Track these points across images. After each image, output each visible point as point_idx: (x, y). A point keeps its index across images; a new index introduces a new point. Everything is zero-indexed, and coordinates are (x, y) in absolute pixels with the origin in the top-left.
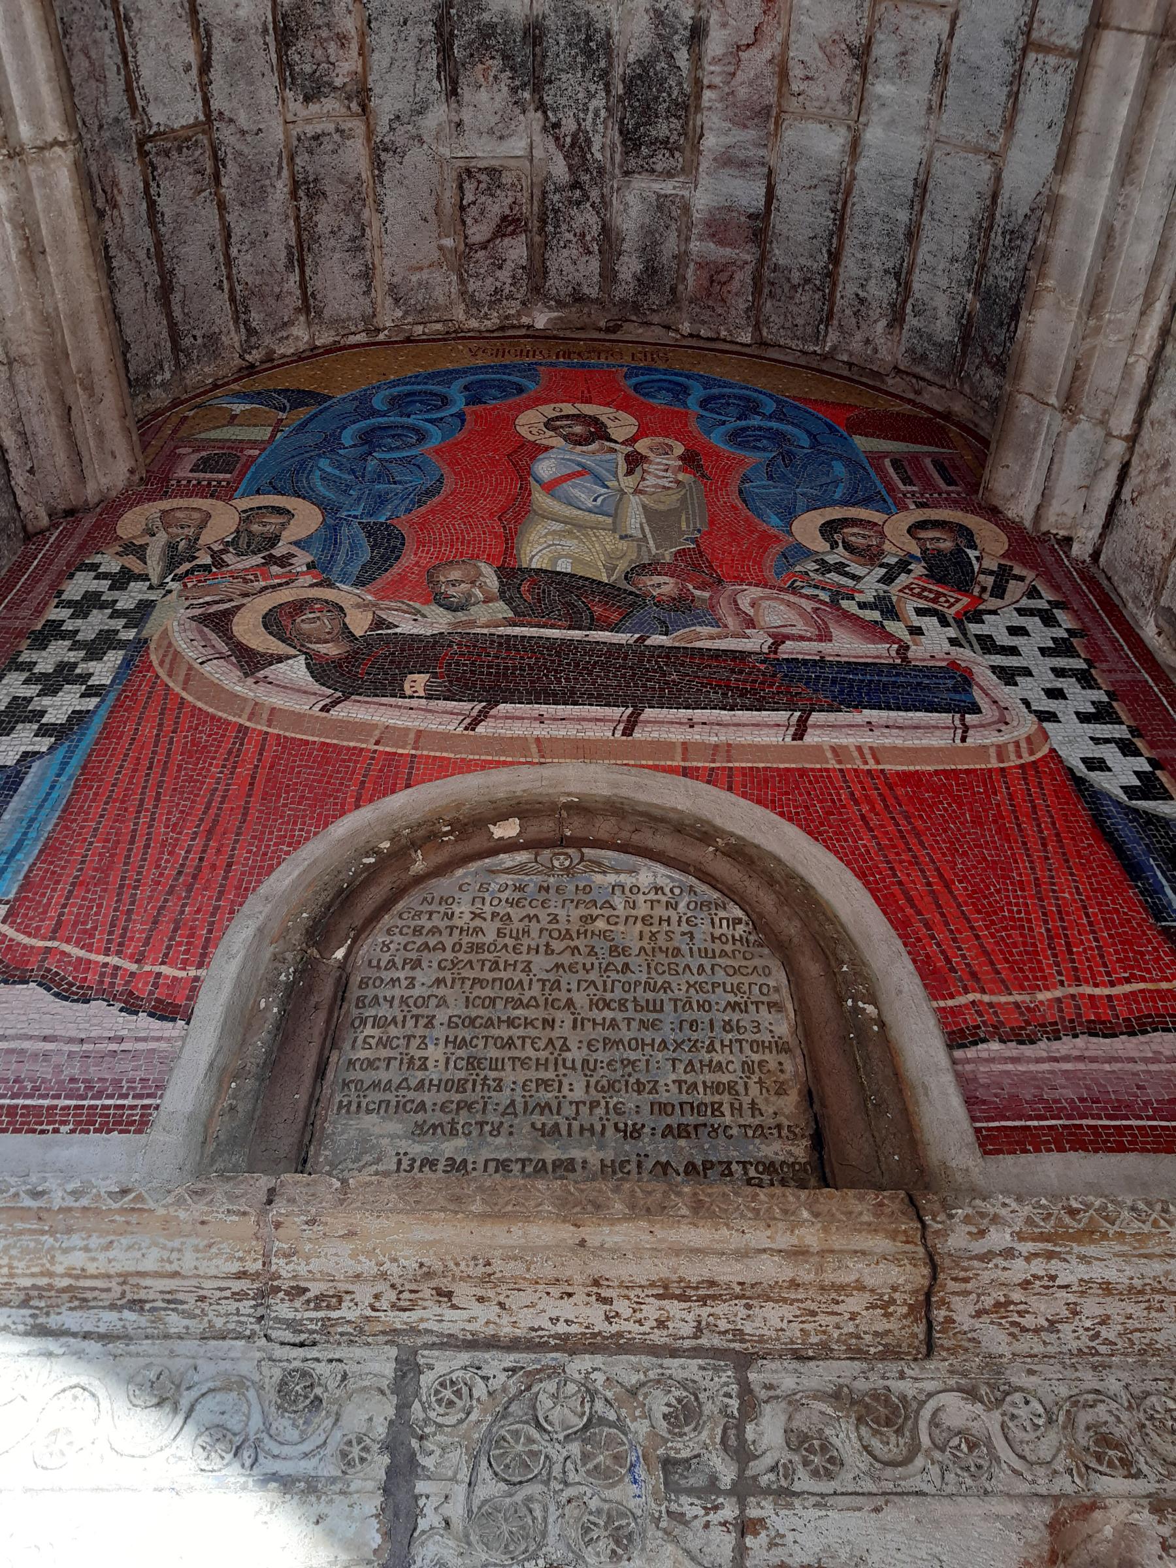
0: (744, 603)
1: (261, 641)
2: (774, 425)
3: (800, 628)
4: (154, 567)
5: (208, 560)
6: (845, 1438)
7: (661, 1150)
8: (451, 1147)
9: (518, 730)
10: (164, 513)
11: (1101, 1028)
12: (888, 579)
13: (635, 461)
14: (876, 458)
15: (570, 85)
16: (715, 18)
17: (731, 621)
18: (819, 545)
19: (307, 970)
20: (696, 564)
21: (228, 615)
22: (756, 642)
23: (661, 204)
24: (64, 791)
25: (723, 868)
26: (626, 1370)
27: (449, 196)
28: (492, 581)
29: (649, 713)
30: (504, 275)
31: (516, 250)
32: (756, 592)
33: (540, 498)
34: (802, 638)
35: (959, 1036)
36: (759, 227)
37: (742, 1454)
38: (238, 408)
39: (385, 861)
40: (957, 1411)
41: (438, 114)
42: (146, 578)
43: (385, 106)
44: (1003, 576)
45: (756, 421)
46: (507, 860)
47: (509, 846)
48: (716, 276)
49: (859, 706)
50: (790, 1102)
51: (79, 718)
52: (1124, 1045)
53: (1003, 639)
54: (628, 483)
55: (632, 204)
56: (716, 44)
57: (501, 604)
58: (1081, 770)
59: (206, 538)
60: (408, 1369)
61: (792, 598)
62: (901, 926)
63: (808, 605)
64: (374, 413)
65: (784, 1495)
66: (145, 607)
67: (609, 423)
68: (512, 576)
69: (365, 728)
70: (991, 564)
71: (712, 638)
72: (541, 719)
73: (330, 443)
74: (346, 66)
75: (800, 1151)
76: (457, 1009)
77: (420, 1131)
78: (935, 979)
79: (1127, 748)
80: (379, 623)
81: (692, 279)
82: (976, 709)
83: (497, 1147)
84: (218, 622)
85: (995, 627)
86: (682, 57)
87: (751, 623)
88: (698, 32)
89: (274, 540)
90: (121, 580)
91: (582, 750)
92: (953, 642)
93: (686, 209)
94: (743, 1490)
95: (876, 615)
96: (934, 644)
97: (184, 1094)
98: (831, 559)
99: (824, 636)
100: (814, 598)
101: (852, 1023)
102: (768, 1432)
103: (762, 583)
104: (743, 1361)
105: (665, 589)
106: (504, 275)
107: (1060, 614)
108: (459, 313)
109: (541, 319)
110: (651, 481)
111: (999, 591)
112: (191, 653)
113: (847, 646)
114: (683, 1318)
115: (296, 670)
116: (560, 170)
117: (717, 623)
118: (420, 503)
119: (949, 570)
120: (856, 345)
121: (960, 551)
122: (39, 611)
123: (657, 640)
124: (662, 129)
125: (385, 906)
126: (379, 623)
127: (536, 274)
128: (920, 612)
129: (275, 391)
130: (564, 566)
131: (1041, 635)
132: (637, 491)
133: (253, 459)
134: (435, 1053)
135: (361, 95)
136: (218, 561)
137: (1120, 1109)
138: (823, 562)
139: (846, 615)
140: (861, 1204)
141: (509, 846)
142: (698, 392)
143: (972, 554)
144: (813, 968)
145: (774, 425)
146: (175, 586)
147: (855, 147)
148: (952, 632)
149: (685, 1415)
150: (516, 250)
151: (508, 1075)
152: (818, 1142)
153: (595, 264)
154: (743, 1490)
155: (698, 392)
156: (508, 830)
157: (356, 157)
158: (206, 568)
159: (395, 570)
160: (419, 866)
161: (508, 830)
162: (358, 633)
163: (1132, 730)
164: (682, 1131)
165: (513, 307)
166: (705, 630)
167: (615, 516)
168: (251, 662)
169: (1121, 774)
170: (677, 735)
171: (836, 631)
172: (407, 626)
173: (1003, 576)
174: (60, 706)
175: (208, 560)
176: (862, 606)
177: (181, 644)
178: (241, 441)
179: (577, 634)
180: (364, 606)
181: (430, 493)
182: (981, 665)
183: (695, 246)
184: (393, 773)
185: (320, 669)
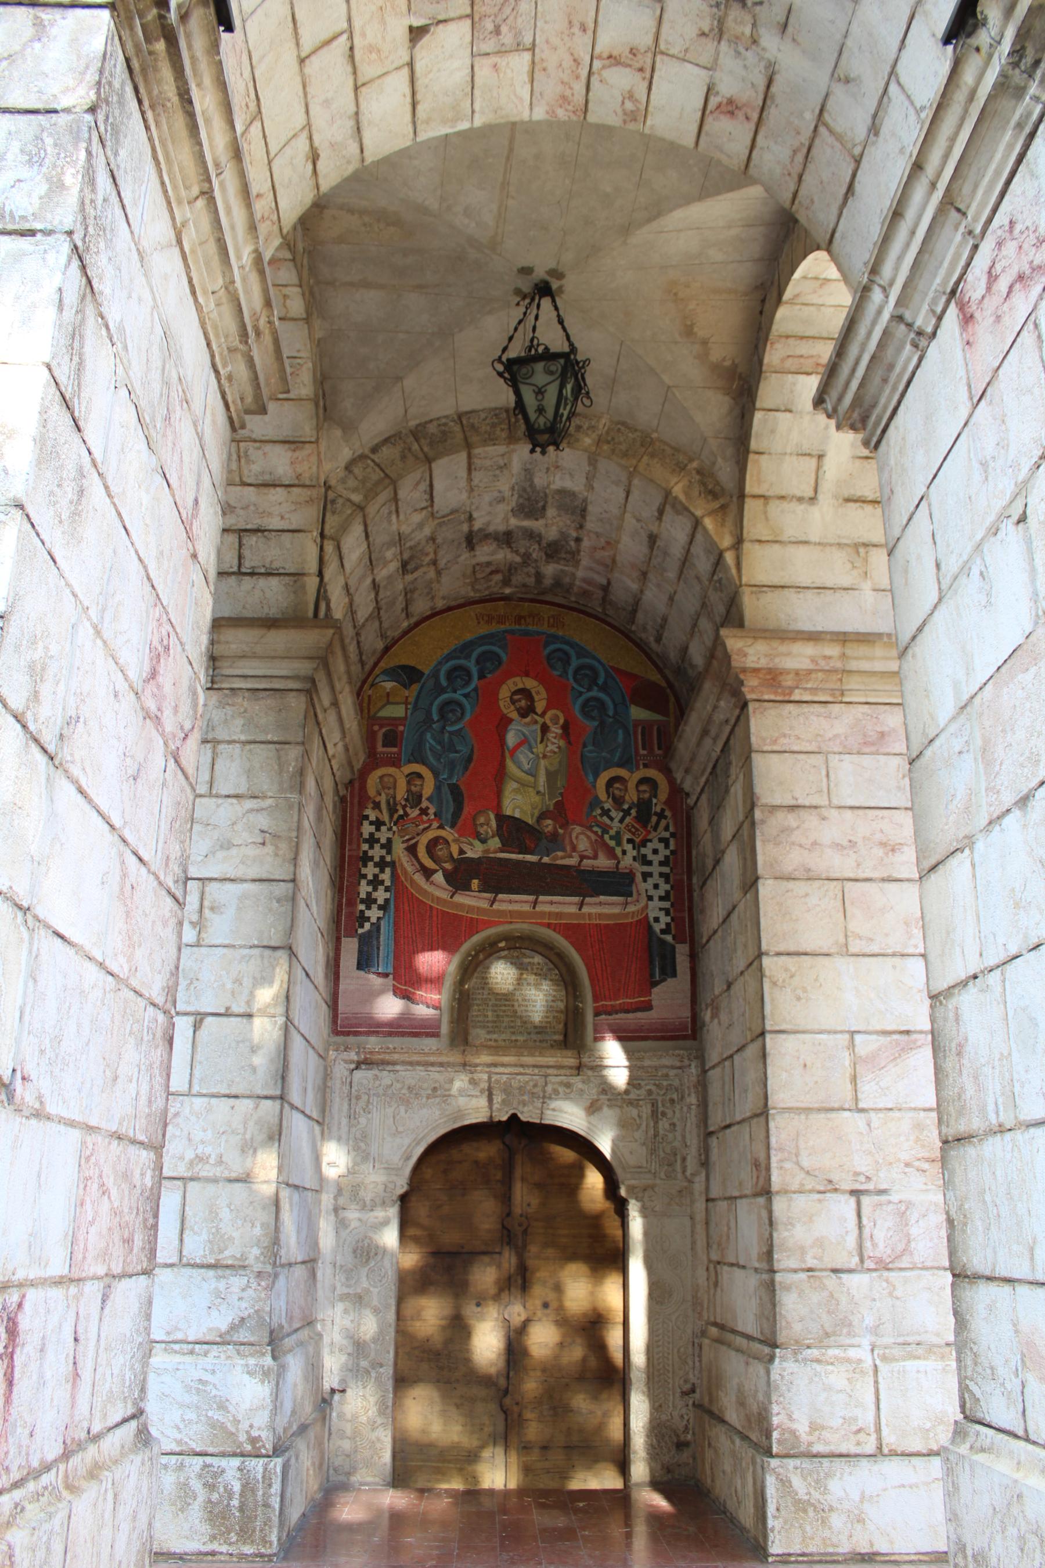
0: (574, 835)
1: (429, 863)
2: (602, 696)
3: (590, 853)
4: (386, 817)
5: (401, 812)
6: (561, 1089)
7: (534, 1037)
8: (495, 1036)
9: (504, 907)
10: (381, 778)
11: (627, 1011)
12: (621, 821)
13: (545, 729)
14: (637, 723)
15: (523, 545)
16: (585, 539)
17: (568, 848)
18: (602, 795)
19: (461, 993)
20: (560, 813)
21: (415, 845)
22: (573, 861)
23: (562, 571)
24: (392, 933)
25: (555, 959)
26: (527, 1078)
27: (469, 571)
28: (494, 823)
29: (541, 898)
30: (493, 583)
31: (498, 577)
32: (578, 829)
33: (511, 766)
34: (588, 858)
35: (597, 1014)
36: (606, 588)
37: (544, 1092)
38: (389, 685)
39: (474, 957)
40: (580, 1085)
41: (465, 555)
42: (384, 824)
43: (442, 563)
44: (661, 815)
45: (595, 693)
46: (503, 953)
47: (502, 949)
48: (585, 593)
49: (598, 895)
50: (561, 1026)
51: (387, 901)
52: (630, 1016)
53: (651, 857)
54: (541, 747)
55: (550, 570)
56: (586, 543)
57: (497, 839)
58: (651, 920)
59: (399, 797)
60: (490, 1078)
61: (589, 833)
62: (592, 980)
63: (593, 837)
64: (440, 690)
65: (550, 1098)
66: (389, 840)
67: (536, 698)
68: (501, 818)
69: (461, 906)
70: (658, 810)
71: (562, 858)
72: (510, 902)
73: (428, 720)
74: (427, 559)
75: (560, 1038)
76: (493, 1002)
77: (489, 1033)
78: (596, 998)
79: (667, 913)
80: (462, 852)
81: (576, 589)
82: (631, 895)
83: (504, 1037)
84: (412, 850)
85: (647, 851)
86: (572, 543)
87: (574, 848)
88: (578, 540)
89: (421, 796)
90: (378, 824)
91: (521, 915)
92: (634, 859)
93: (573, 574)
94: (544, 1097)
95: (612, 843)
96: (627, 862)
97: (445, 1029)
98: (607, 806)
99: (595, 857)
100: (596, 833)
101: (576, 1008)
102: (549, 1088)
103: (582, 826)
104: (546, 1076)
105: (550, 828)
106: (493, 583)
107: (672, 842)
108: (472, 594)
109: (507, 591)
110: (550, 747)
111: (655, 829)
112: (410, 869)
113: (603, 862)
114: (536, 1071)
115: (439, 877)
116: (518, 559)
117: (564, 850)
118: (466, 768)
119: (644, 812)
120: (643, 636)
121: (650, 801)
122: (359, 846)
123: (546, 860)
124: (563, 555)
125: (475, 970)
126: (462, 852)
127: (506, 582)
128: (629, 841)
129: (399, 667)
130: (517, 815)
131: (664, 852)
132: (545, 756)
133: (402, 732)
134: (490, 1013)
135: (434, 563)
136: (406, 814)
137: (625, 1031)
138: (602, 808)
139: (605, 845)
140: (569, 1053)
141: (502, 949)
142: (575, 663)
143: (654, 801)
144: (570, 988)
145: (602, 696)
146: (395, 828)
147: (642, 591)
148: (635, 853)
149: (535, 1086)
150: (498, 577)
151: (506, 1019)
152: (565, 1036)
153: (533, 579)
154: (544, 1097)
155: (575, 663)
156: (502, 944)
157: (432, 574)
158: (401, 817)
159: (463, 817)
160: (481, 956)
161: (502, 944)
162: (456, 856)
163: (672, 905)
164: (538, 1033)
165: (495, 590)
166: (560, 854)
167: (534, 776)
168: (428, 873)
169: (665, 919)
170: (547, 908)
171: (601, 855)
172: (470, 854)
173: (661, 815)
174: (381, 895)
175: (401, 812)
176: (611, 838)
177: (406, 864)
178: (395, 719)
179: (520, 857)
180: (455, 841)
181: (470, 759)
182: (639, 868)
183: (577, 583)
184: (473, 926)
185: (449, 877)
